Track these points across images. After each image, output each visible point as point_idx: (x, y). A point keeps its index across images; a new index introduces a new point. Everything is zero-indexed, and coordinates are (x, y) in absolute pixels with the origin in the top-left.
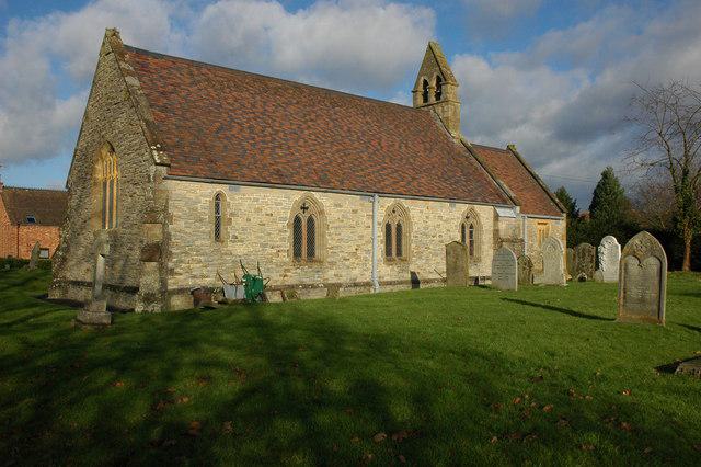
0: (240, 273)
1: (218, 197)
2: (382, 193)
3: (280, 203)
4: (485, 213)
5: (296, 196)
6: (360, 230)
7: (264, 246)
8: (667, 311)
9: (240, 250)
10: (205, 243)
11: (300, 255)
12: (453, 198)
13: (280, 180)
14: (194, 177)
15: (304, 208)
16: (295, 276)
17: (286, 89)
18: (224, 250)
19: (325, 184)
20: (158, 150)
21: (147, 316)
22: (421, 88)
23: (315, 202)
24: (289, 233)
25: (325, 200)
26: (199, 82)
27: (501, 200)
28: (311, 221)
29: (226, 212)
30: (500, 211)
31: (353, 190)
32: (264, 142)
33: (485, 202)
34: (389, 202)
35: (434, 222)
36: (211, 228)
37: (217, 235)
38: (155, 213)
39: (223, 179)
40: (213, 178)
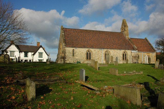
0: (77, 61)
1: (73, 50)
2: (104, 48)
3: (84, 50)
4: (129, 52)
5: (87, 49)
6: (100, 55)
7: (81, 57)
8: (92, 85)
9: (77, 58)
10: (71, 56)
11: (88, 59)
12: (120, 49)
13: (84, 47)
14: (70, 47)
15: (89, 51)
16: (86, 62)
17: (91, 32)
18: (74, 58)
19: (92, 47)
20: (64, 43)
21: (79, 64)
22: (122, 28)
23: (90, 50)
24: (85, 55)
25: (92, 50)
26: (75, 32)
27: (133, 49)
28: (90, 53)
29: (75, 52)
30: (132, 51)
31: (98, 48)
32: (83, 41)
33: (128, 49)
34: (106, 50)
35: (116, 54)
36: (72, 54)
37: (73, 55)
38: (64, 52)
39: (74, 47)
40: (72, 47)
